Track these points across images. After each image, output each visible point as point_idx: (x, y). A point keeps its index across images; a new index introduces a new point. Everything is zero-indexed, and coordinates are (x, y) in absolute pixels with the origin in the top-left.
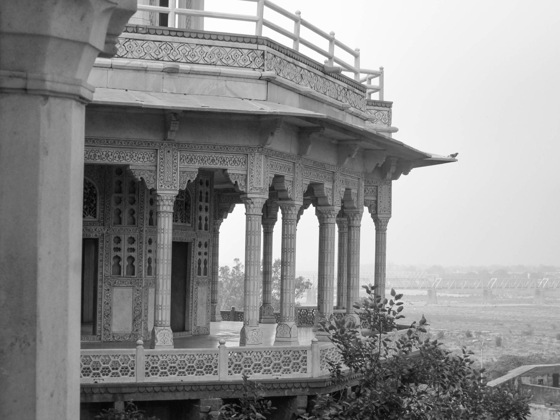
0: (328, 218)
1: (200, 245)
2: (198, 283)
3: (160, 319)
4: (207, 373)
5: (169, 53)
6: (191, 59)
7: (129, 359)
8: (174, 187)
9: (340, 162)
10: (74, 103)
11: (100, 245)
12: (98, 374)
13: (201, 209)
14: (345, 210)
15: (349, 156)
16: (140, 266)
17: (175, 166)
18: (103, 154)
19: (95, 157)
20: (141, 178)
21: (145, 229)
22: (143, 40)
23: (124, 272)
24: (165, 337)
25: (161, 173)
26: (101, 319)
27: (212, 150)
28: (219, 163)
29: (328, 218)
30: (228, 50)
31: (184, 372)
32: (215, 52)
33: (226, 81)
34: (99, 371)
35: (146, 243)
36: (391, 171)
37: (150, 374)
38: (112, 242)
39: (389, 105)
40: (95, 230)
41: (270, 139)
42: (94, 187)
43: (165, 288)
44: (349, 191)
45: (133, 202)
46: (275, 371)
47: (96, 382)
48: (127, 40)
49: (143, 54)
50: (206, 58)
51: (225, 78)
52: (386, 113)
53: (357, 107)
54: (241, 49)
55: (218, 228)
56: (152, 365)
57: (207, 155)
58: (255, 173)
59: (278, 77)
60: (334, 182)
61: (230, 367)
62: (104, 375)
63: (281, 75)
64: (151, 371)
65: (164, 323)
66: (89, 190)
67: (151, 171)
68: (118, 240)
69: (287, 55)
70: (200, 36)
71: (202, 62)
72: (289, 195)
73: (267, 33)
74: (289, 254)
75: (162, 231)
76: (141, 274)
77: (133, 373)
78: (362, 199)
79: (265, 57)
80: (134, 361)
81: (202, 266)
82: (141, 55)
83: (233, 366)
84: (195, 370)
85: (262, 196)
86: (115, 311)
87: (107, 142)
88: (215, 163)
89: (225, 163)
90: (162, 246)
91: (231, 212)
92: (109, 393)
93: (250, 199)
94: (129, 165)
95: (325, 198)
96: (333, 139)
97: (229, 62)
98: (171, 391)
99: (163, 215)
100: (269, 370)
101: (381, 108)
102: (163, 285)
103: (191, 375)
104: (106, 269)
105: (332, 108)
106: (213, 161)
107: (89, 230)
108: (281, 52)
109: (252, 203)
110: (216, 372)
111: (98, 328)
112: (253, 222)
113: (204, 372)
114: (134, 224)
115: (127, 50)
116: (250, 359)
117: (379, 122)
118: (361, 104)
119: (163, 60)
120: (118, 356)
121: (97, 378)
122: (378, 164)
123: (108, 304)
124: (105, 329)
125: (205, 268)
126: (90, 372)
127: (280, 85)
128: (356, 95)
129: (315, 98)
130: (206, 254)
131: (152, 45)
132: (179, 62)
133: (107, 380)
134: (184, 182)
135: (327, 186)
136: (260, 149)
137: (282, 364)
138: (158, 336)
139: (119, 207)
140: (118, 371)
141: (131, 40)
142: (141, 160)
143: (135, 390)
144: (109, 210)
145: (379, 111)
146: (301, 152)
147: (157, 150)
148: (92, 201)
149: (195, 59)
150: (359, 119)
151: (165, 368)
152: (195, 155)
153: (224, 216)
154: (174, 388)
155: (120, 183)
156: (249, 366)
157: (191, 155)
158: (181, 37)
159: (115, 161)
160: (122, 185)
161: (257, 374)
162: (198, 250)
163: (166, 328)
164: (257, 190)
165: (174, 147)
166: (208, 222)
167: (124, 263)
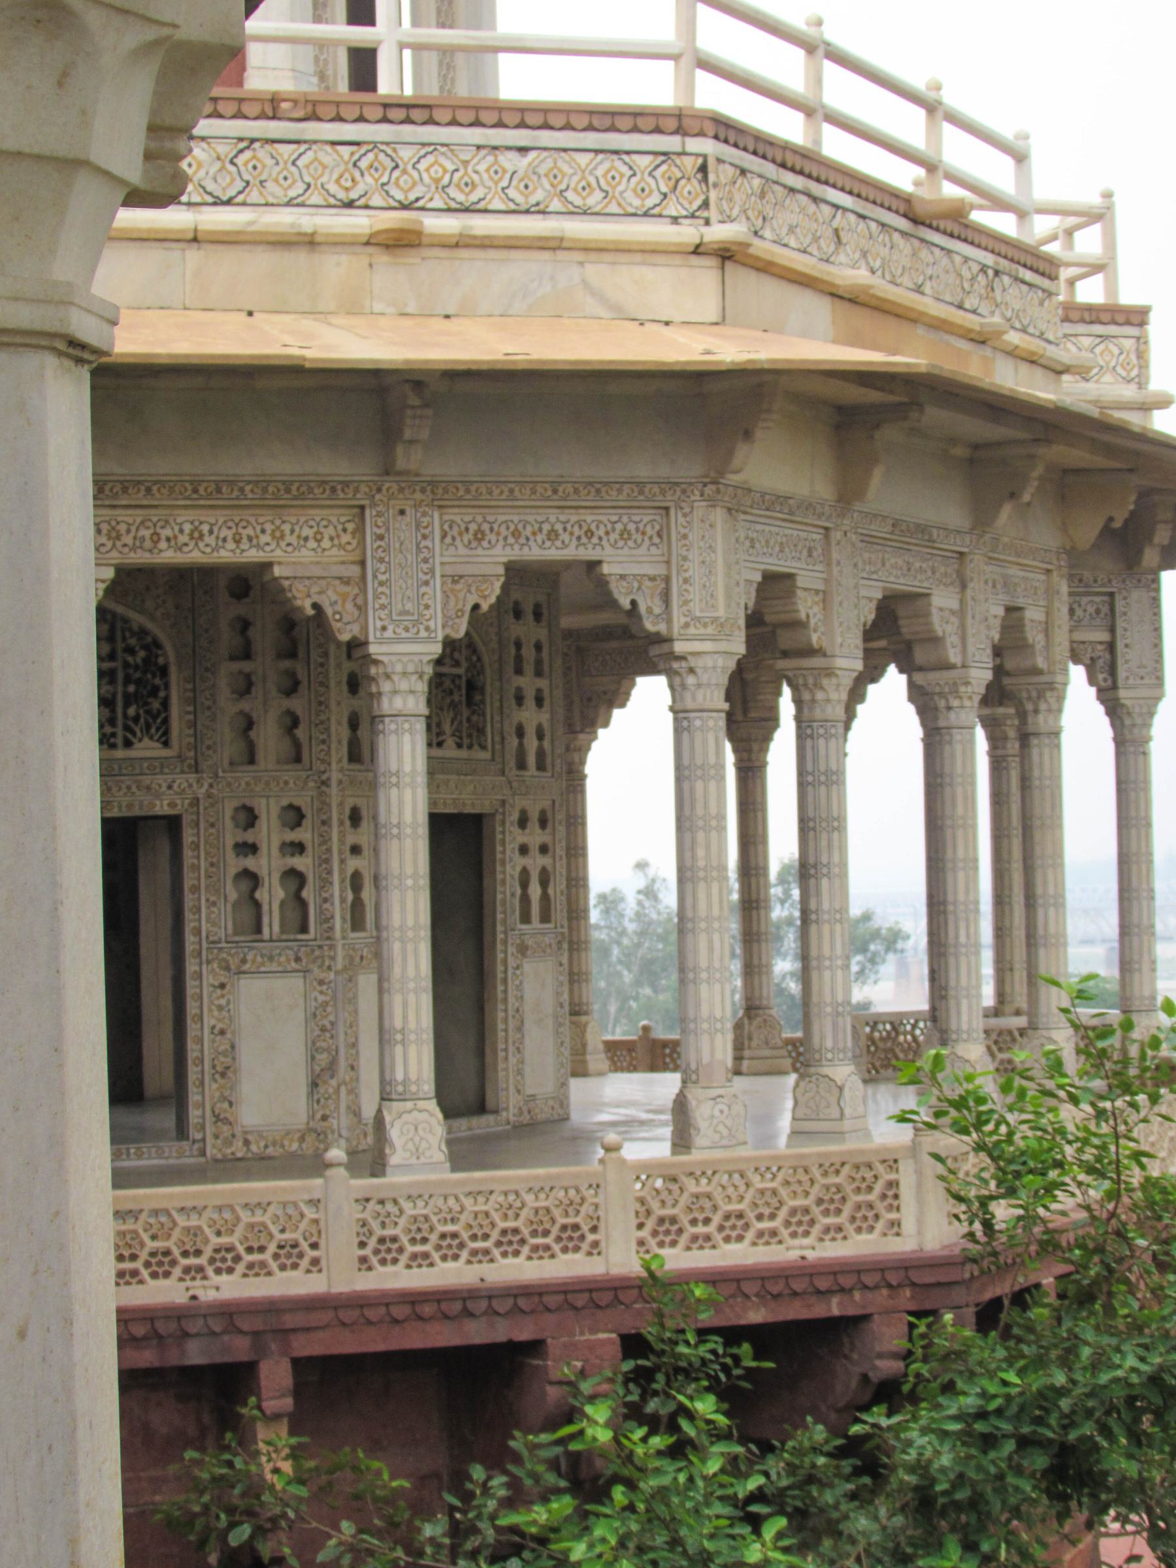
0: (949, 708)
1: (523, 822)
2: (523, 950)
3: (400, 1076)
4: (565, 1250)
5: (385, 179)
6: (460, 197)
7: (302, 1215)
8: (427, 629)
9: (982, 519)
10: (51, 361)
11: (188, 836)
12: (200, 1269)
13: (520, 699)
14: (1006, 681)
15: (1012, 495)
16: (325, 900)
17: (426, 561)
18: (181, 531)
19: (156, 543)
20: (315, 606)
21: (335, 776)
22: (297, 142)
23: (272, 923)
24: (419, 1133)
25: (381, 584)
26: (202, 1083)
27: (548, 499)
28: (574, 542)
29: (949, 708)
30: (583, 159)
31: (487, 1252)
32: (542, 170)
33: (581, 264)
34: (202, 1261)
35: (341, 823)
36: (1156, 540)
37: (374, 1260)
38: (229, 823)
39: (1136, 317)
40: (170, 787)
41: (741, 450)
42: (157, 644)
43: (411, 972)
44: (1015, 615)
45: (292, 688)
46: (794, 1235)
47: (194, 1297)
48: (242, 145)
49: (299, 188)
50: (512, 193)
51: (578, 256)
52: (1128, 344)
53: (1031, 330)
54: (628, 153)
55: (583, 762)
56: (379, 1232)
57: (531, 518)
58: (694, 570)
59: (756, 242)
60: (964, 587)
61: (640, 1226)
62: (218, 1271)
63: (767, 233)
64: (376, 1252)
65: (413, 1088)
66: (142, 654)
67: (346, 581)
68: (249, 817)
69: (783, 165)
70: (488, 117)
71: (497, 205)
72: (814, 638)
73: (714, 96)
74: (824, 836)
75: (394, 780)
76: (331, 929)
77: (315, 1262)
78: (1062, 639)
79: (712, 178)
80: (316, 1221)
81: (535, 891)
82: (292, 193)
83: (650, 1224)
84: (523, 1241)
85: (723, 646)
86: (248, 1056)
87: (195, 491)
88: (558, 543)
89: (595, 540)
90: (395, 831)
91: (623, 705)
92: (241, 1332)
93: (682, 658)
95: (935, 641)
96: (953, 441)
97: (591, 201)
98: (447, 1317)
99: (393, 727)
100: (774, 1233)
101: (1112, 330)
102: (405, 959)
103: (510, 1260)
104: (210, 916)
105: (946, 337)
106: (553, 535)
107: (148, 788)
108: (764, 157)
109: (691, 671)
110: (595, 1244)
111: (194, 1114)
112: (698, 736)
113: (556, 1248)
114: (298, 759)
115: (246, 177)
116: (709, 1196)
117: (1108, 378)
118: (1045, 318)
119: (367, 207)
120: (263, 1206)
121: (198, 1283)
122: (1111, 519)
123: (222, 1032)
124: (217, 1118)
125: (545, 897)
126: (173, 1263)
127: (766, 268)
128: (1025, 288)
129: (887, 307)
130: (544, 849)
131: (327, 156)
132: (423, 209)
133: (229, 1287)
134: (459, 613)
135: (943, 600)
136: (709, 490)
137: (816, 1211)
138: (394, 1134)
139: (245, 705)
140: (267, 1256)
141: (257, 145)
142: (312, 544)
143: (327, 1316)
144: (213, 718)
145: (1103, 338)
146: (848, 494)
147: (362, 508)
148: (154, 691)
149: (474, 198)
150: (1039, 372)
151: (424, 1240)
152: (490, 518)
153: (601, 719)
154: (458, 1306)
155: (244, 625)
156: (707, 1221)
157: (479, 519)
158: (424, 123)
160: (251, 632)
161: (733, 1247)
162: (520, 837)
163: (421, 1104)
164: (705, 625)
165: (418, 496)
166: (546, 744)
167: (273, 894)
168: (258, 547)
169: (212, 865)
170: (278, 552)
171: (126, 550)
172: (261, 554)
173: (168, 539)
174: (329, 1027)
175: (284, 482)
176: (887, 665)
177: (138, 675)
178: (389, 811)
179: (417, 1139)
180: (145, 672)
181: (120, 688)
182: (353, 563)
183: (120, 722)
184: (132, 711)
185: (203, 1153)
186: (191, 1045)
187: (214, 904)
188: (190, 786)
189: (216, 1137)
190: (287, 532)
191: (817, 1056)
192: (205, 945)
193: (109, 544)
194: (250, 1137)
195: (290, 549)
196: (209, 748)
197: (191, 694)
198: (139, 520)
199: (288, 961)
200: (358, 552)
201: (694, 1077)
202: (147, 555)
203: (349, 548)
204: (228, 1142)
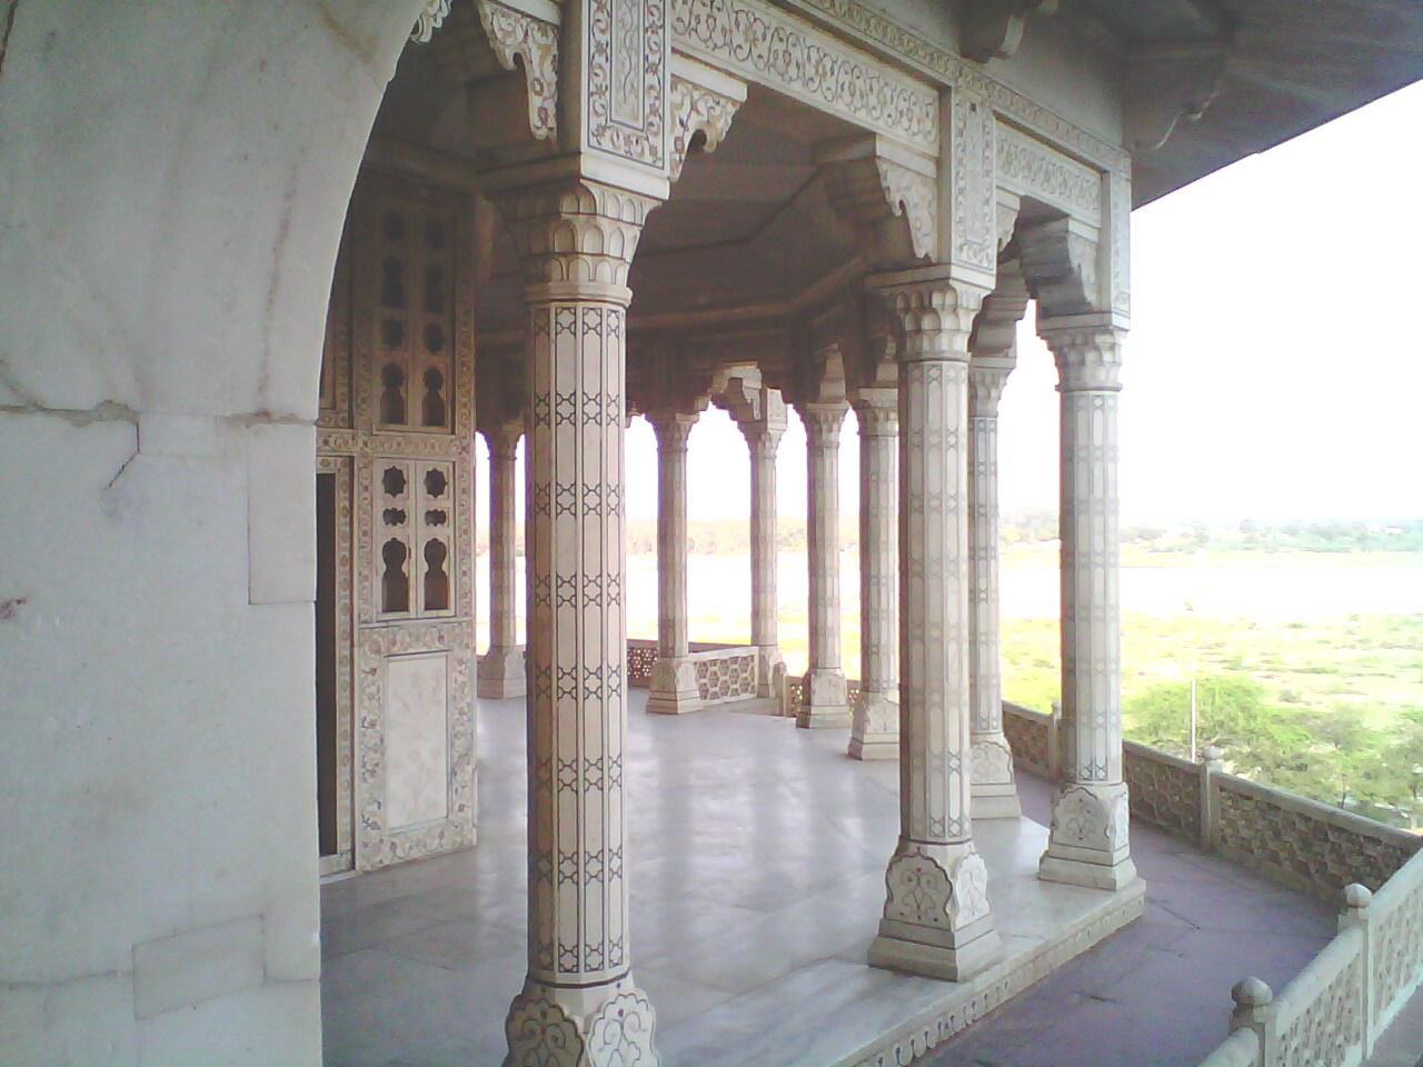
16: (464, 573)
23: (417, 594)
86: (396, 748)
94: (869, 136)
104: (365, 590)
123: (373, 725)
152: (1015, 141)
165: (983, 92)
168: (869, 113)
170: (881, 123)
171: (761, 64)
172: (869, 120)
174: (466, 710)
179: (919, 894)
185: (353, 866)
186: (342, 745)
187: (366, 578)
189: (366, 845)
193: (746, 47)
194: (394, 840)
199: (432, 640)
200: (936, 147)
204: (378, 848)
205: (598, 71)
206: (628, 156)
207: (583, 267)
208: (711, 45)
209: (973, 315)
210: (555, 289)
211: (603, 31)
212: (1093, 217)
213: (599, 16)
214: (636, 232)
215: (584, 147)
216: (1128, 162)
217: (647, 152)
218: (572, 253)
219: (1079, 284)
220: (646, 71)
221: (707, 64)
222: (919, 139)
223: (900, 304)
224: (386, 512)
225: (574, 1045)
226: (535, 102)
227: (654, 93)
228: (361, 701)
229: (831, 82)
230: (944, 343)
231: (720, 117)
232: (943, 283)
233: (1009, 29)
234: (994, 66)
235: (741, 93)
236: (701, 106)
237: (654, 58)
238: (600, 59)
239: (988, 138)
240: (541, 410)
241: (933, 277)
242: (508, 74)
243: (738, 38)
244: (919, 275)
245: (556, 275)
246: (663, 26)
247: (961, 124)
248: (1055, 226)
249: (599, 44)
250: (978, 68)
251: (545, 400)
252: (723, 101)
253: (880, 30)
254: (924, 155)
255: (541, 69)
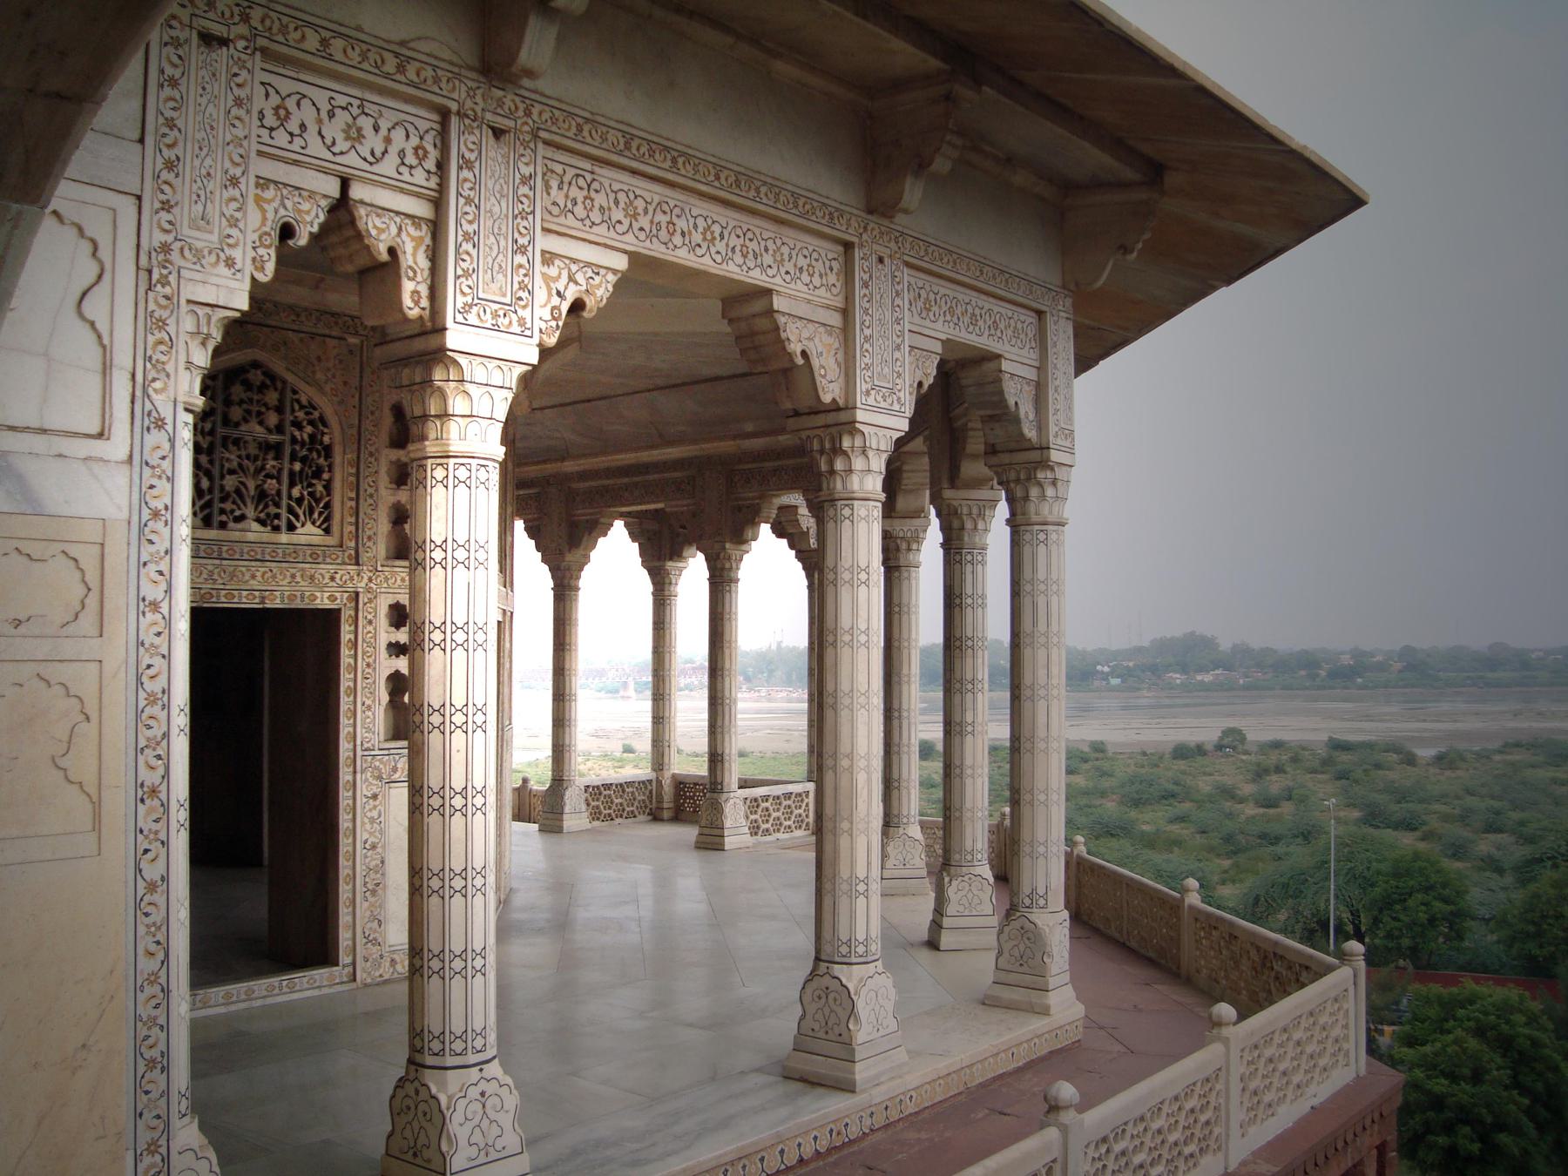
11: (346, 634)
40: (332, 579)
75: (863, 576)
87: (718, 178)
91: (605, 534)
94: (767, 293)
111: (344, 937)
123: (374, 847)
139: (403, 496)
142: (805, 278)
144: (375, 507)
148: (317, 474)
152: (936, 289)
159: (732, 267)
165: (892, 245)
168: (763, 270)
169: (368, 665)
170: (778, 280)
171: (642, 236)
172: (764, 277)
173: (683, 234)
175: (793, 193)
176: (598, 528)
177: (304, 452)
178: (854, 613)
180: (310, 450)
181: (287, 465)
182: (836, 309)
183: (284, 502)
184: (296, 492)
187: (369, 708)
188: (352, 579)
190: (786, 257)
191: (969, 857)
192: (359, 753)
193: (626, 222)
195: (788, 278)
196: (369, 538)
197: (353, 479)
198: (657, 199)
201: (1042, 902)
202: (662, 248)
203: (835, 291)
205: (465, 257)
206: (496, 328)
207: (453, 428)
208: (588, 222)
209: (885, 456)
210: (431, 448)
211: (470, 222)
212: (1031, 356)
213: (467, 209)
214: (510, 396)
215: (449, 323)
216: (1069, 302)
217: (515, 323)
218: (444, 416)
219: (1017, 421)
220: (514, 252)
221: (584, 240)
222: (822, 292)
223: (816, 446)
224: (390, 645)
225: (437, 1119)
226: (408, 286)
227: (522, 271)
228: (363, 824)
229: (720, 246)
230: (855, 483)
231: (600, 286)
232: (851, 427)
233: (907, 186)
234: (900, 218)
235: (621, 263)
236: (580, 277)
237: (522, 241)
238: (467, 246)
239: (899, 288)
240: (419, 556)
241: (838, 421)
242: (384, 265)
243: (617, 215)
244: (831, 418)
245: (432, 435)
246: (533, 212)
247: (866, 277)
248: (992, 365)
249: (466, 234)
250: (886, 222)
251: (422, 547)
252: (602, 272)
253: (771, 196)
254: (828, 307)
255: (414, 258)
